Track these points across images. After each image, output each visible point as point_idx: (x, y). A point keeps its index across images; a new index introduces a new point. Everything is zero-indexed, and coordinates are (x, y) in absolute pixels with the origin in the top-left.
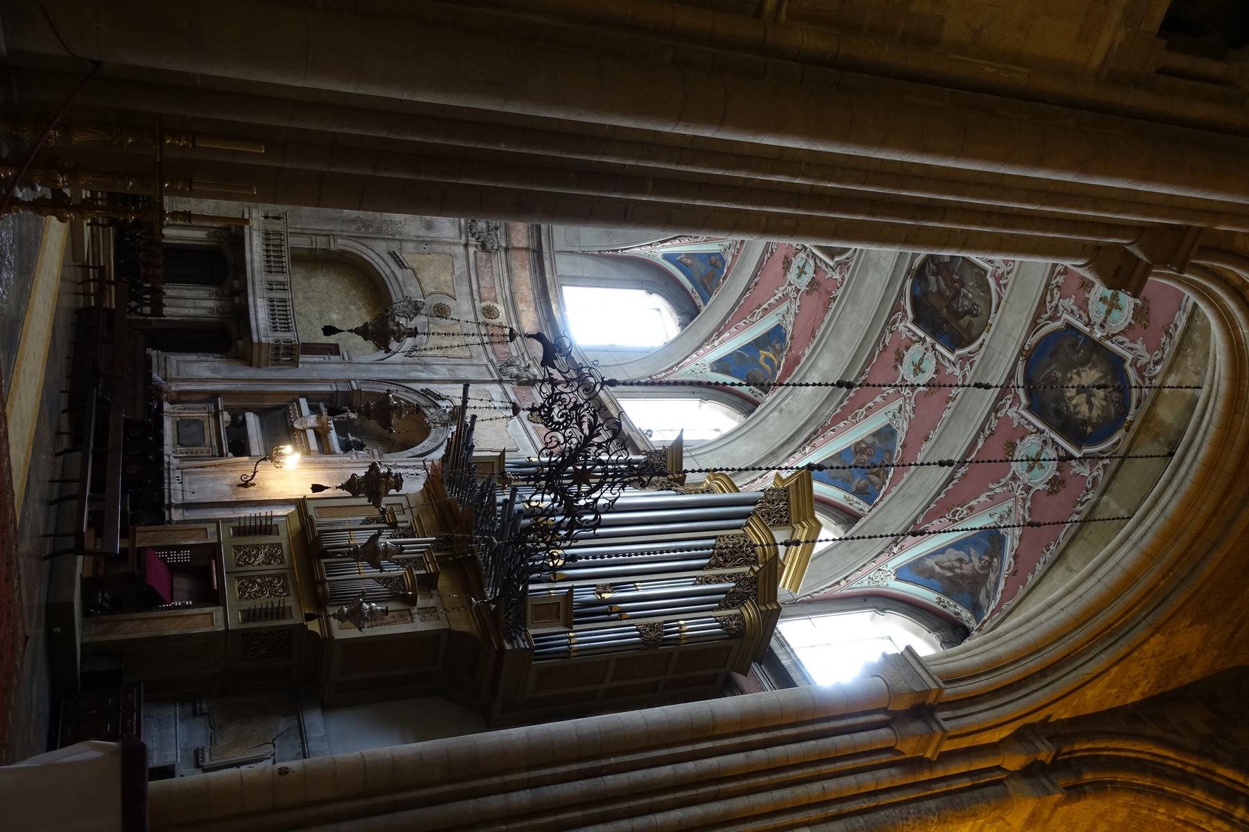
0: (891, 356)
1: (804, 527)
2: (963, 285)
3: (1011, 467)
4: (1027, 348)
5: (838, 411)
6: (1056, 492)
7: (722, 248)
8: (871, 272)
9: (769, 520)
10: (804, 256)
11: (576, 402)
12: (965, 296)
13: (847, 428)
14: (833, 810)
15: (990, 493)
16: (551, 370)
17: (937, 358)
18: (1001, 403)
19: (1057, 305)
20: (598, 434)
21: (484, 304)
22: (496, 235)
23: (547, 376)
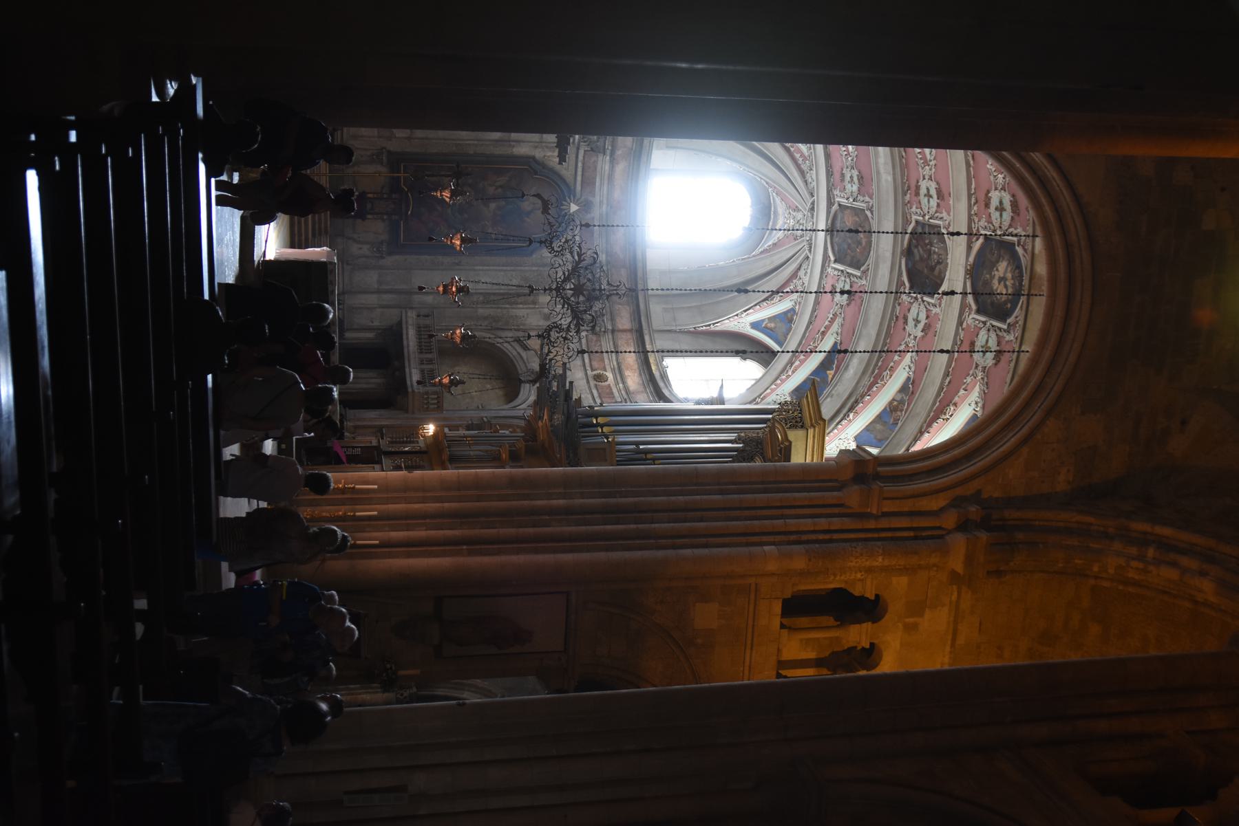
0: (901, 321)
1: (814, 427)
2: (932, 246)
3: (974, 360)
4: (969, 267)
5: (872, 379)
6: (999, 361)
7: (793, 303)
8: (881, 266)
9: (786, 424)
10: (843, 278)
11: (566, 239)
12: (934, 252)
13: (879, 389)
14: (793, 537)
15: (964, 387)
16: (548, 217)
17: (926, 307)
18: (964, 317)
19: (978, 228)
20: (584, 260)
21: (595, 372)
22: (603, 321)
23: (546, 222)
